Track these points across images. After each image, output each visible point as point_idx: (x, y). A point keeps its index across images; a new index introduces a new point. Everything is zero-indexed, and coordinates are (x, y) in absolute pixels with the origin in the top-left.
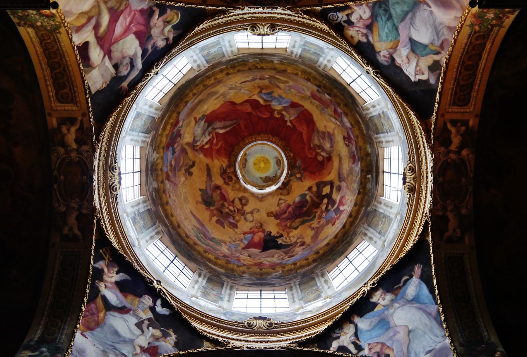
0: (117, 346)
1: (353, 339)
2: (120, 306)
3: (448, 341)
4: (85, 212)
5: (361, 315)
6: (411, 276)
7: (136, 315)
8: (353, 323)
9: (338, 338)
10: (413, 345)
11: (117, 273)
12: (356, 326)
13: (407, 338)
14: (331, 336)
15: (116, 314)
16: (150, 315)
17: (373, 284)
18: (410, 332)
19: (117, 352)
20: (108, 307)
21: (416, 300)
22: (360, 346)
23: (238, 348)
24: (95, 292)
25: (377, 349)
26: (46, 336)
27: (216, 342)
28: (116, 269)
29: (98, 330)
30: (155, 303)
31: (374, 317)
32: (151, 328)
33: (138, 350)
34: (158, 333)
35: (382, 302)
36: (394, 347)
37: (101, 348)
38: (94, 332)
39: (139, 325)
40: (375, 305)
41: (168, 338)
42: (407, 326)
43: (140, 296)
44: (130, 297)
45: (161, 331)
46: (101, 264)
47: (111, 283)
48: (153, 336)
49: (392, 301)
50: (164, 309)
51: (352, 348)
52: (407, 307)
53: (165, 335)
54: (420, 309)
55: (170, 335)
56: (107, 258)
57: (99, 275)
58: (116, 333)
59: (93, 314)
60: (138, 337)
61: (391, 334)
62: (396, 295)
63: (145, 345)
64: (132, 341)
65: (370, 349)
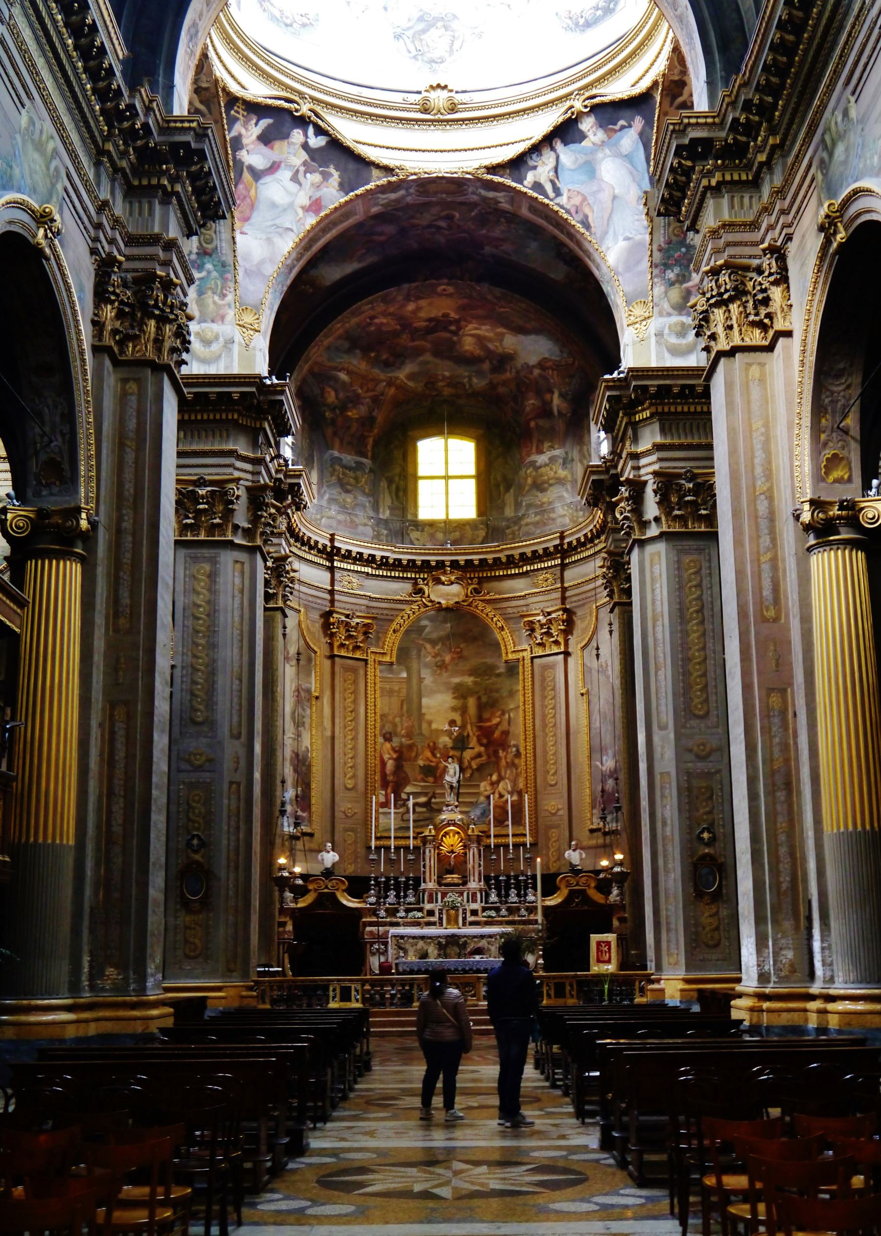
0: (277, 222)
1: (552, 174)
2: (269, 165)
3: (648, 238)
4: (204, 85)
5: (566, 143)
6: (630, 126)
7: (290, 167)
8: (553, 149)
9: (535, 168)
10: (616, 218)
11: (256, 124)
12: (558, 158)
13: (610, 202)
14: (526, 162)
15: (267, 179)
16: (304, 156)
17: (586, 107)
18: (615, 197)
19: (280, 230)
20: (257, 175)
21: (628, 158)
22: (558, 189)
23: (415, 174)
24: (239, 164)
25: (577, 200)
26: (205, 245)
27: (388, 170)
28: (254, 121)
29: (255, 214)
30: (306, 135)
31: (580, 152)
32: (308, 175)
33: (300, 212)
34: (316, 177)
35: (590, 134)
36: (595, 208)
37: (264, 236)
38: (252, 221)
39: (295, 179)
40: (582, 136)
41: (331, 180)
42: (613, 188)
43: (287, 136)
44: (277, 144)
45: (322, 173)
46: (238, 128)
47: (253, 143)
48: (312, 184)
49: (603, 142)
50: (319, 138)
51: (549, 188)
52: (618, 161)
53: (326, 176)
54: (631, 173)
55: (330, 175)
56: (240, 117)
57: (237, 143)
58: (274, 205)
59: (245, 198)
60: (296, 195)
61: (595, 188)
62: (610, 138)
63: (306, 202)
64: (291, 205)
65: (569, 198)
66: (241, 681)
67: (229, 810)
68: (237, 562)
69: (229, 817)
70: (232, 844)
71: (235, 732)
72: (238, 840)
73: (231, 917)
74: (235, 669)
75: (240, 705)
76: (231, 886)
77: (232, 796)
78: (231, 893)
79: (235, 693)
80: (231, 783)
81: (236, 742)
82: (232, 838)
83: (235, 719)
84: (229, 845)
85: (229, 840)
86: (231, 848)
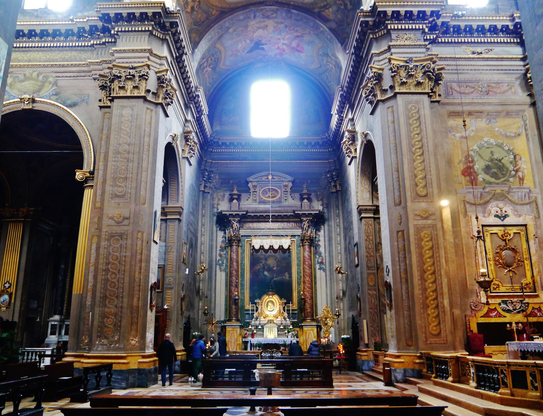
66: (398, 172)
67: (398, 248)
68: (389, 108)
69: (399, 253)
70: (402, 267)
71: (397, 201)
72: (406, 265)
73: (406, 312)
74: (393, 166)
75: (399, 185)
76: (404, 293)
77: (399, 239)
78: (404, 297)
79: (395, 180)
80: (398, 232)
81: (398, 207)
82: (402, 264)
83: (397, 194)
84: (400, 269)
85: (400, 266)
86: (402, 270)
